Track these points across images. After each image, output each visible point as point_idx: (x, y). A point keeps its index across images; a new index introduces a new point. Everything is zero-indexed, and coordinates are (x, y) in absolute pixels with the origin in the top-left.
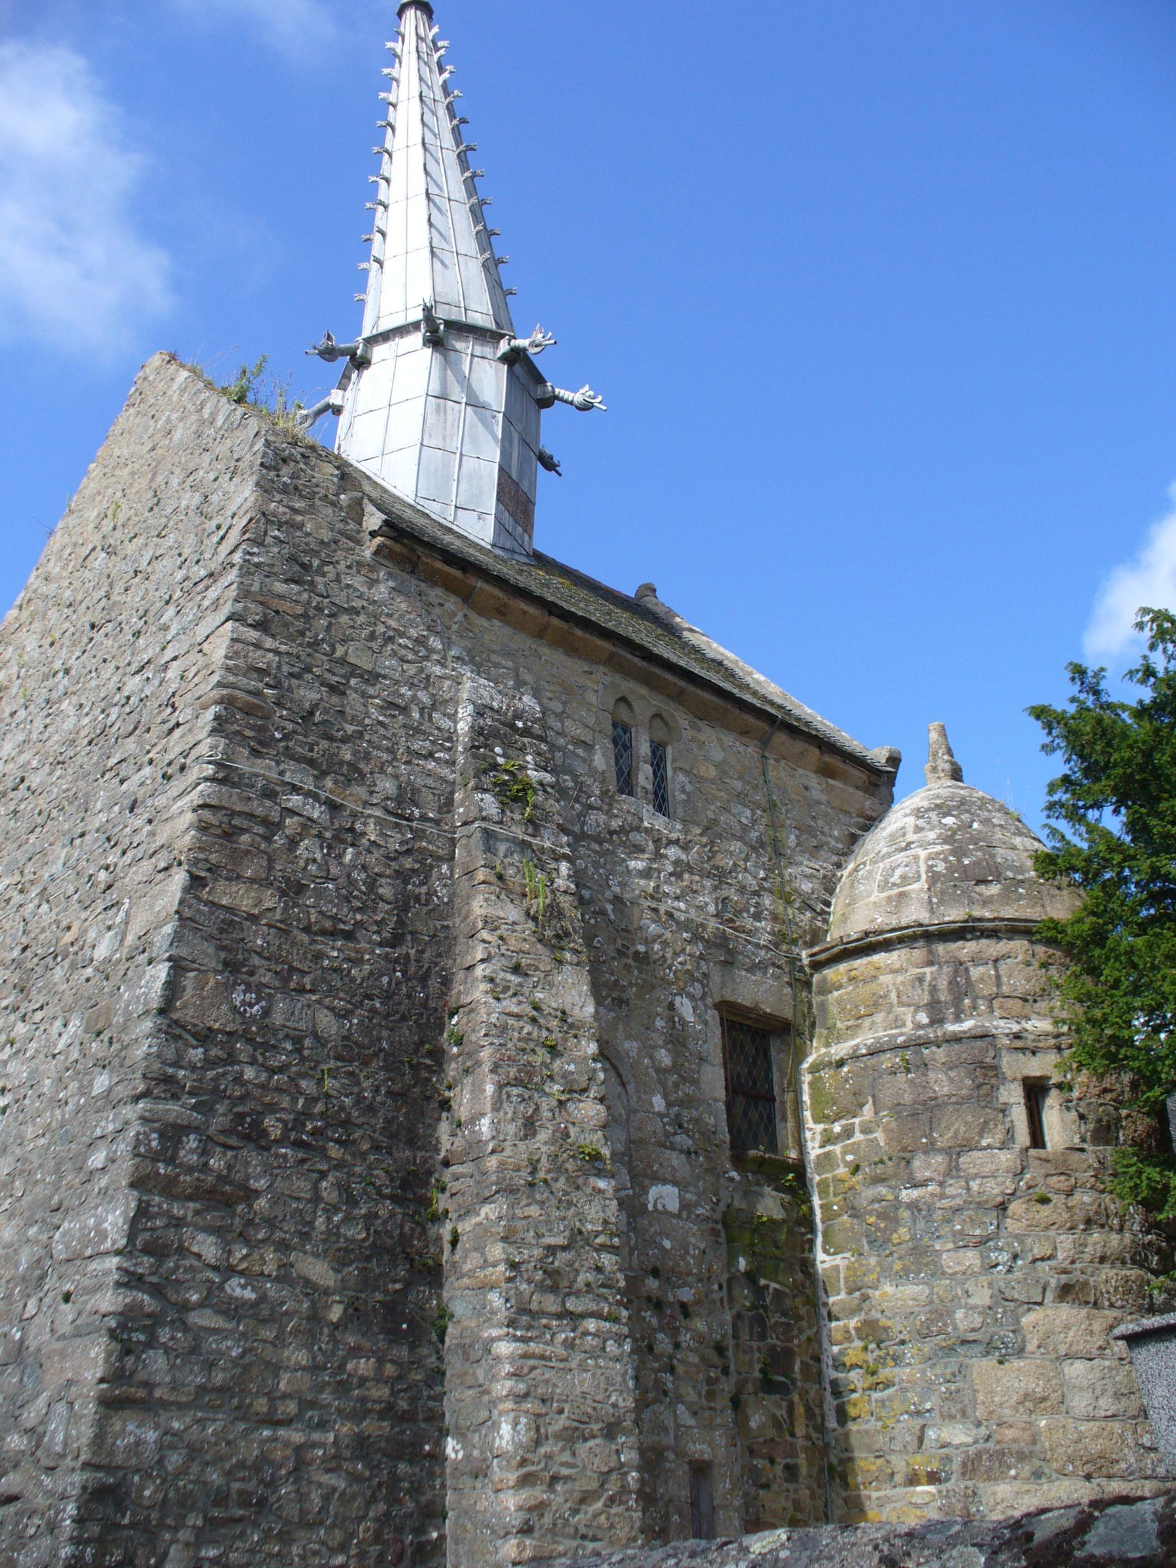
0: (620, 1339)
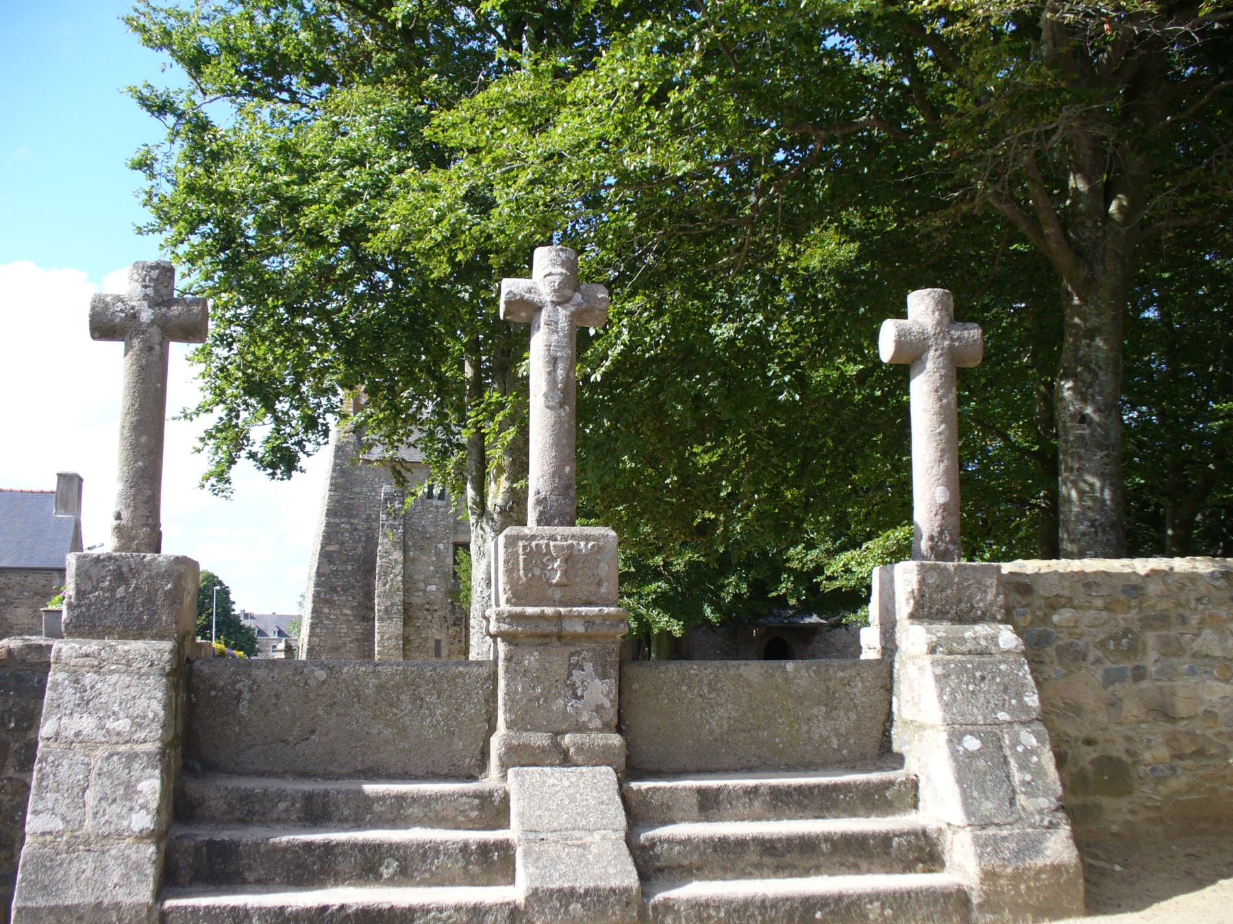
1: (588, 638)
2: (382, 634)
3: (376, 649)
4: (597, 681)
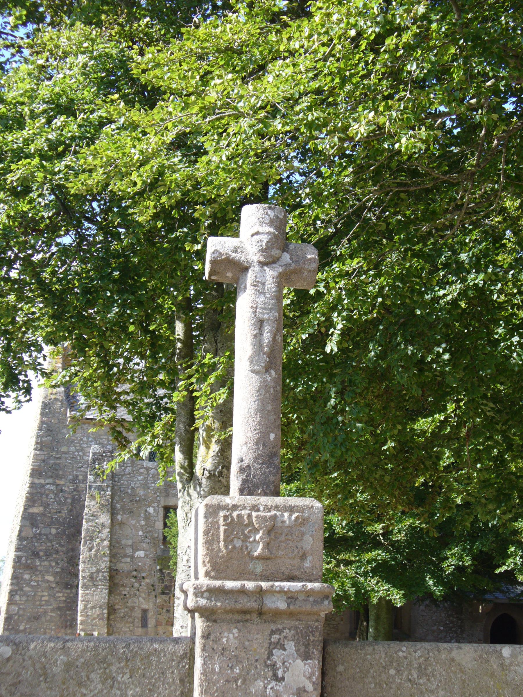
0: (106, 589)
1: (291, 615)
2: (86, 602)
3: (79, 618)
4: (299, 661)
